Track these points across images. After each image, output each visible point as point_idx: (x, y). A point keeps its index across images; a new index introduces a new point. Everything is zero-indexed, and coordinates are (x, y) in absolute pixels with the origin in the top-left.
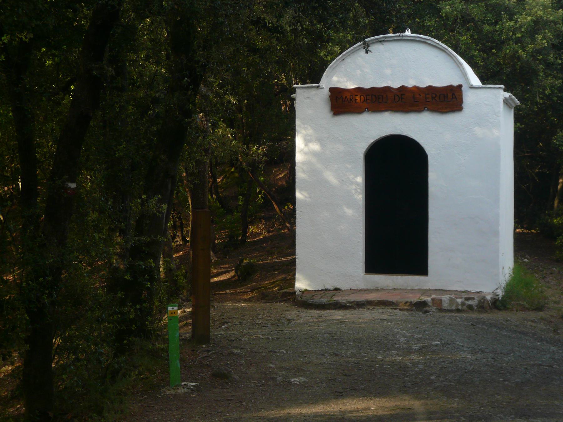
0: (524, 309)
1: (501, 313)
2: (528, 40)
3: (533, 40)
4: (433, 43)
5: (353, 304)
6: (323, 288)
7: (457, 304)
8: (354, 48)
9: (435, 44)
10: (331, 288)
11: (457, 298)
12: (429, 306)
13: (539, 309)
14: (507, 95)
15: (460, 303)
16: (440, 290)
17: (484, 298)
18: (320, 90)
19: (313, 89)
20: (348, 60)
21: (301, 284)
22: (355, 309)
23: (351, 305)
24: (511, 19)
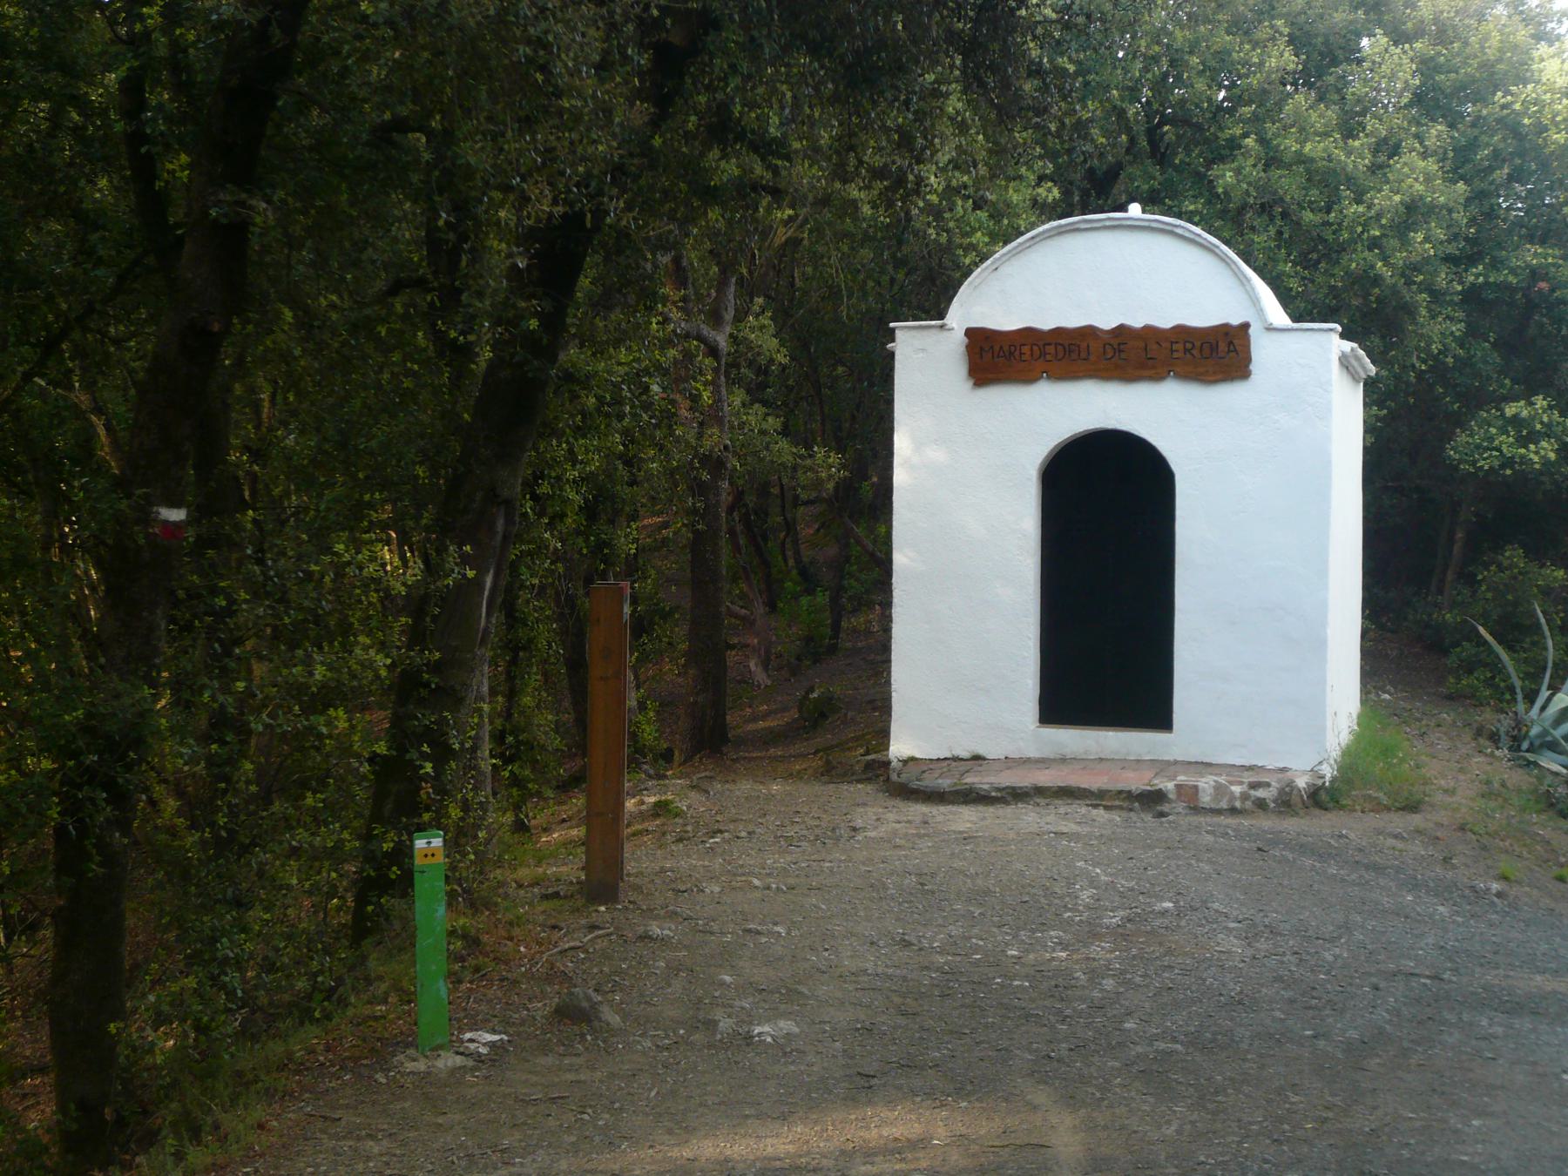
0: (1379, 808)
1: (1329, 815)
2: (1395, 243)
3: (1405, 242)
4: (1187, 234)
5: (1004, 794)
6: (949, 755)
7: (1232, 797)
8: (1020, 244)
9: (1192, 236)
10: (964, 754)
11: (1232, 783)
12: (1169, 801)
13: (1412, 807)
14: (1348, 346)
15: (1238, 795)
16: (1197, 763)
17: (1291, 784)
18: (945, 334)
19: (933, 331)
20: (1006, 269)
21: (901, 746)
22: (1007, 803)
23: (999, 795)
24: (1359, 202)
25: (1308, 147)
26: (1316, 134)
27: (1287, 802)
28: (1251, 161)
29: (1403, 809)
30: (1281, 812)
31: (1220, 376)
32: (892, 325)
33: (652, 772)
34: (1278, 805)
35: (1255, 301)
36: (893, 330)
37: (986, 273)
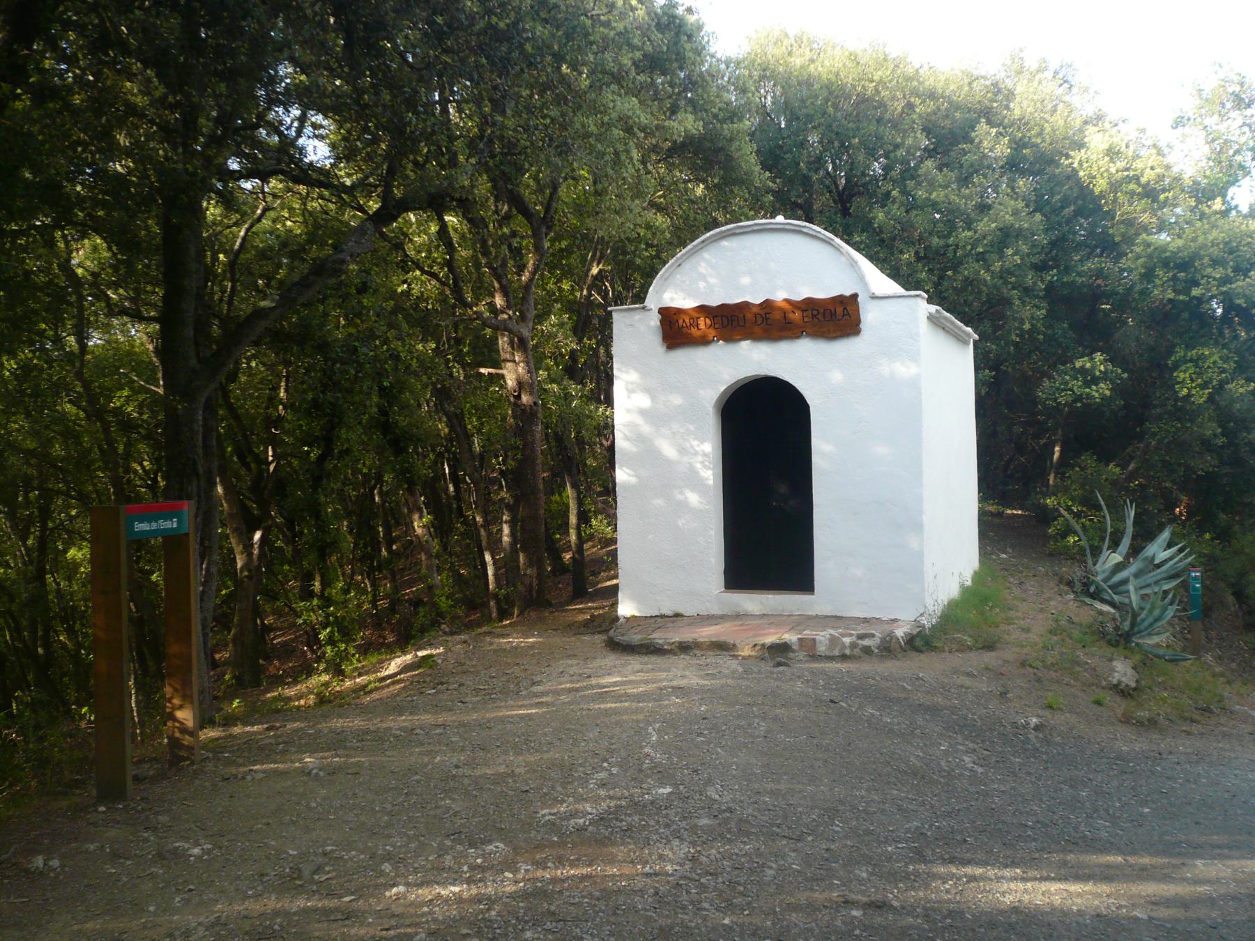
0: (963, 648)
1: (922, 656)
2: (994, 256)
3: (1001, 255)
4: (811, 232)
5: (673, 647)
6: (658, 614)
7: (843, 646)
8: (694, 247)
9: (814, 233)
10: (669, 613)
11: (843, 635)
12: (793, 651)
13: (990, 647)
14: (933, 308)
15: (847, 644)
16: (832, 616)
17: (891, 635)
18: (647, 313)
19: (638, 311)
20: (687, 266)
21: (626, 608)
22: (675, 654)
23: (669, 648)
24: (969, 229)
25: (934, 195)
26: (940, 186)
27: (888, 648)
28: (896, 206)
29: (983, 648)
30: (882, 656)
31: (839, 333)
32: (609, 309)
33: (447, 630)
34: (881, 651)
35: (862, 278)
36: (611, 312)
37: (671, 270)
